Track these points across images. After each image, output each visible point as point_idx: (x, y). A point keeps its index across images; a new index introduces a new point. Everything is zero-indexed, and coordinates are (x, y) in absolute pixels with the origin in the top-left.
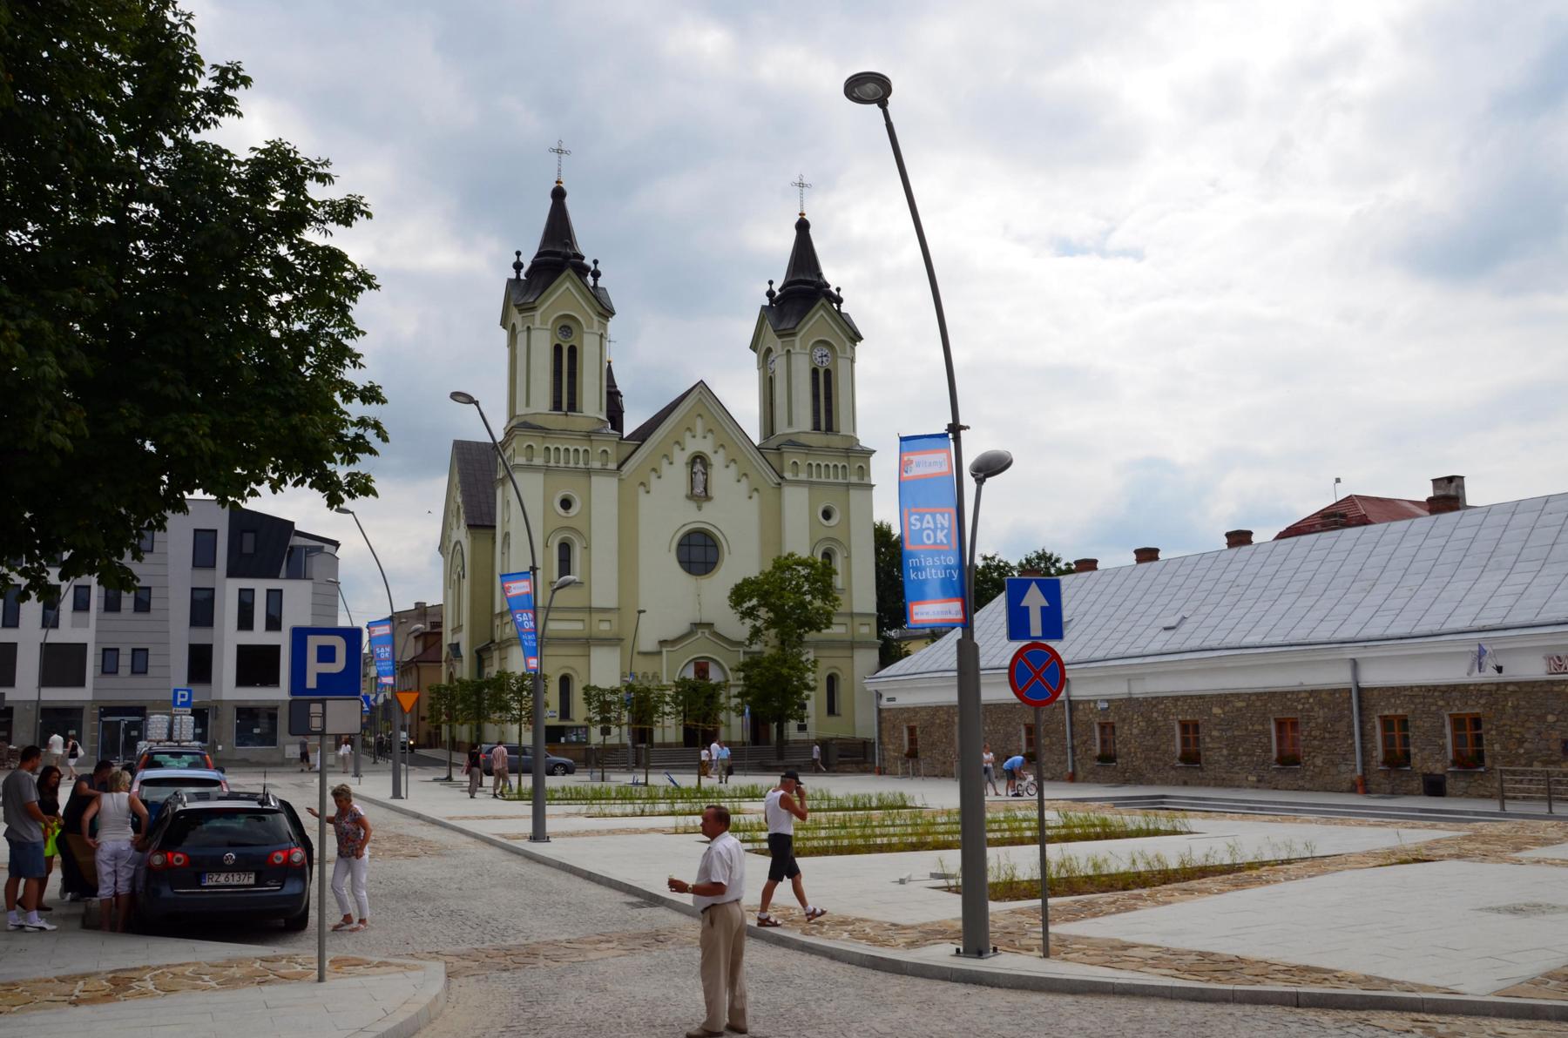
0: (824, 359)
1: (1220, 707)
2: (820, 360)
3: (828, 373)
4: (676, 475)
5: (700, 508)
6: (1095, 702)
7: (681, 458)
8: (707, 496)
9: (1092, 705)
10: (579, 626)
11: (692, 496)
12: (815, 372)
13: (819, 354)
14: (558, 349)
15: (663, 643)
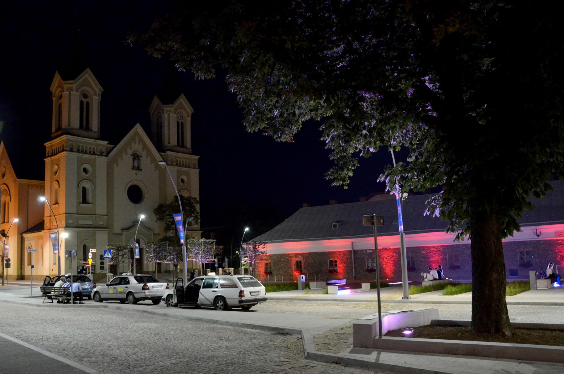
0: (182, 118)
1: (425, 251)
2: (180, 118)
3: (182, 124)
4: (128, 159)
5: (136, 174)
6: (366, 250)
7: (130, 152)
8: (139, 169)
9: (364, 252)
10: (90, 222)
11: (134, 168)
12: (178, 123)
13: (180, 116)
14: (82, 103)
15: (122, 230)
